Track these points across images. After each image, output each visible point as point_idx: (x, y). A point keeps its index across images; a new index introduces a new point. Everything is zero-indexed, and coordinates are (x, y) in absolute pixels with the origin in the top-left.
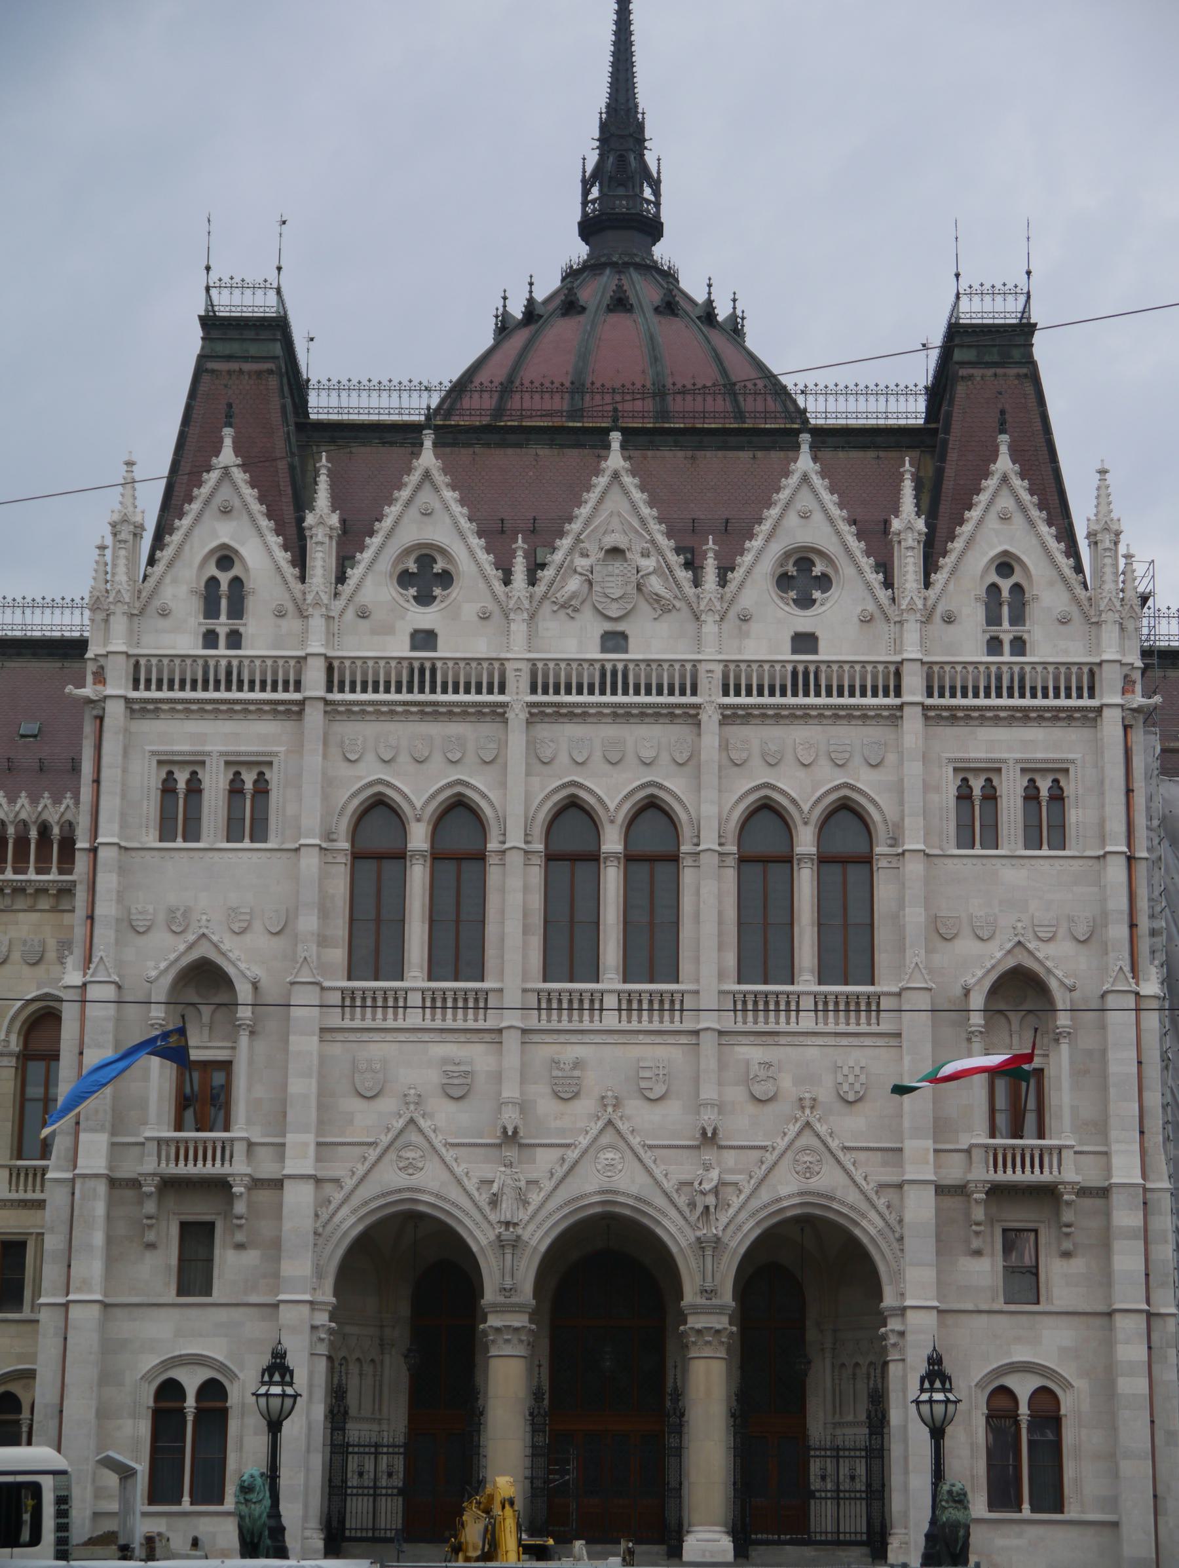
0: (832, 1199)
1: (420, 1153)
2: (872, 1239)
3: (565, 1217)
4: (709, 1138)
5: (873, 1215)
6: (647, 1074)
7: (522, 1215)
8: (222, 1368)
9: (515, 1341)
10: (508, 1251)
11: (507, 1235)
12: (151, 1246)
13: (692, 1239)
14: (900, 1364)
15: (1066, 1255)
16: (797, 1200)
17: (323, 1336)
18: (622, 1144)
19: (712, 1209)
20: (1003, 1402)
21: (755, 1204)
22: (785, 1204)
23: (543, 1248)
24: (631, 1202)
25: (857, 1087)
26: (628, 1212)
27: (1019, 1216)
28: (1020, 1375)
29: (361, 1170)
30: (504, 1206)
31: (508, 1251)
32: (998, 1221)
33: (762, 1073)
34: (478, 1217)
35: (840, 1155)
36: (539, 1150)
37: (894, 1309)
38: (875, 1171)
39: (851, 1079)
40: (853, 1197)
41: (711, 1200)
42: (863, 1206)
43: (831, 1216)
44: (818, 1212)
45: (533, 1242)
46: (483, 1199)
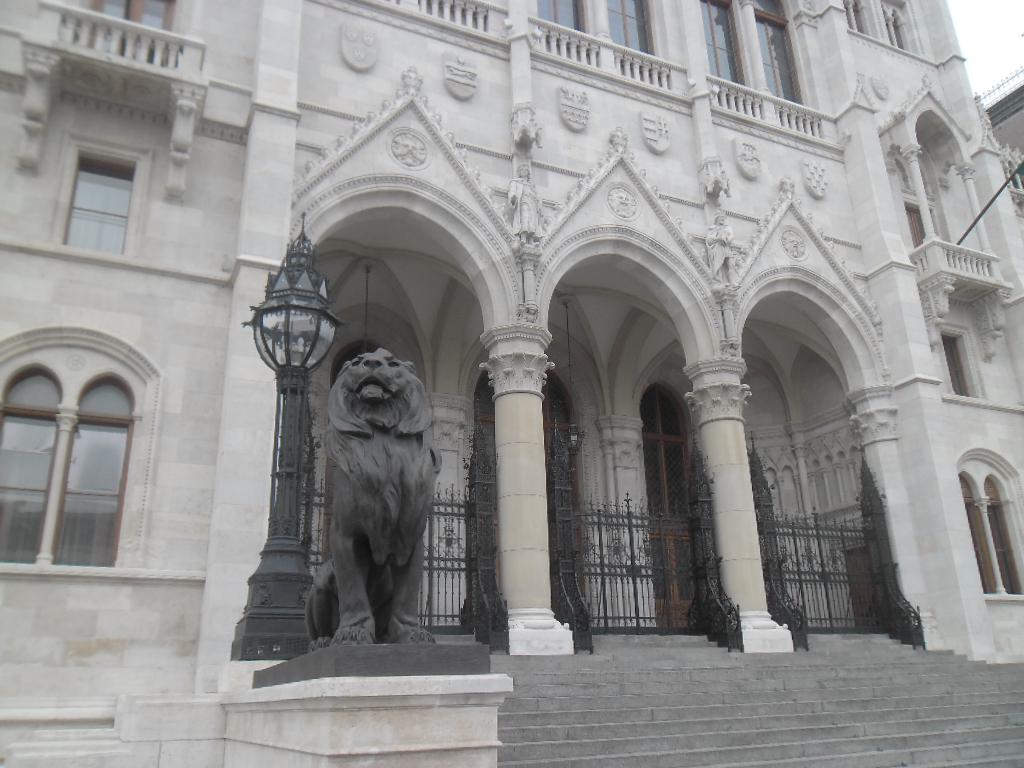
0: (818, 278)
2: (851, 323)
6: (651, 127)
8: (131, 357)
11: (530, 247)
12: (28, 168)
14: (893, 445)
16: (787, 275)
18: (632, 186)
24: (645, 246)
26: (637, 258)
29: (349, 144)
30: (526, 214)
31: (529, 266)
34: (490, 226)
36: (550, 173)
37: (883, 389)
39: (817, 178)
40: (833, 279)
43: (812, 297)
46: (498, 207)
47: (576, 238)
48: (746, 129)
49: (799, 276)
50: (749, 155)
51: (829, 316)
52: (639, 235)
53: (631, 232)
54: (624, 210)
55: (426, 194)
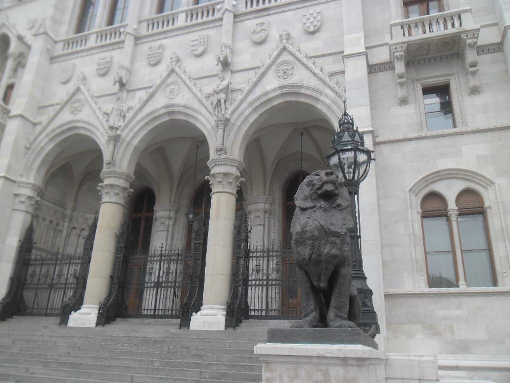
1: (81, 103)
3: (147, 124)
4: (225, 64)
5: (328, 91)
6: (195, 43)
7: (121, 123)
9: (112, 193)
10: (112, 142)
13: (214, 123)
15: (475, 91)
16: (279, 92)
17: (23, 199)
18: (180, 81)
19: (222, 101)
20: (434, 205)
21: (251, 98)
22: (271, 96)
23: (135, 142)
24: (181, 110)
25: (315, 23)
26: (182, 117)
27: (434, 75)
28: (446, 181)
32: (418, 80)
33: (259, 29)
35: (305, 61)
38: (330, 65)
39: (312, 20)
40: (313, 82)
41: (222, 96)
42: (321, 87)
43: (302, 99)
44: (293, 99)
45: (128, 139)
47: (143, 118)
48: (264, 13)
49: (286, 90)
50: (259, 29)
51: (316, 107)
52: (178, 106)
53: (173, 106)
54: (172, 95)
55: (80, 125)
